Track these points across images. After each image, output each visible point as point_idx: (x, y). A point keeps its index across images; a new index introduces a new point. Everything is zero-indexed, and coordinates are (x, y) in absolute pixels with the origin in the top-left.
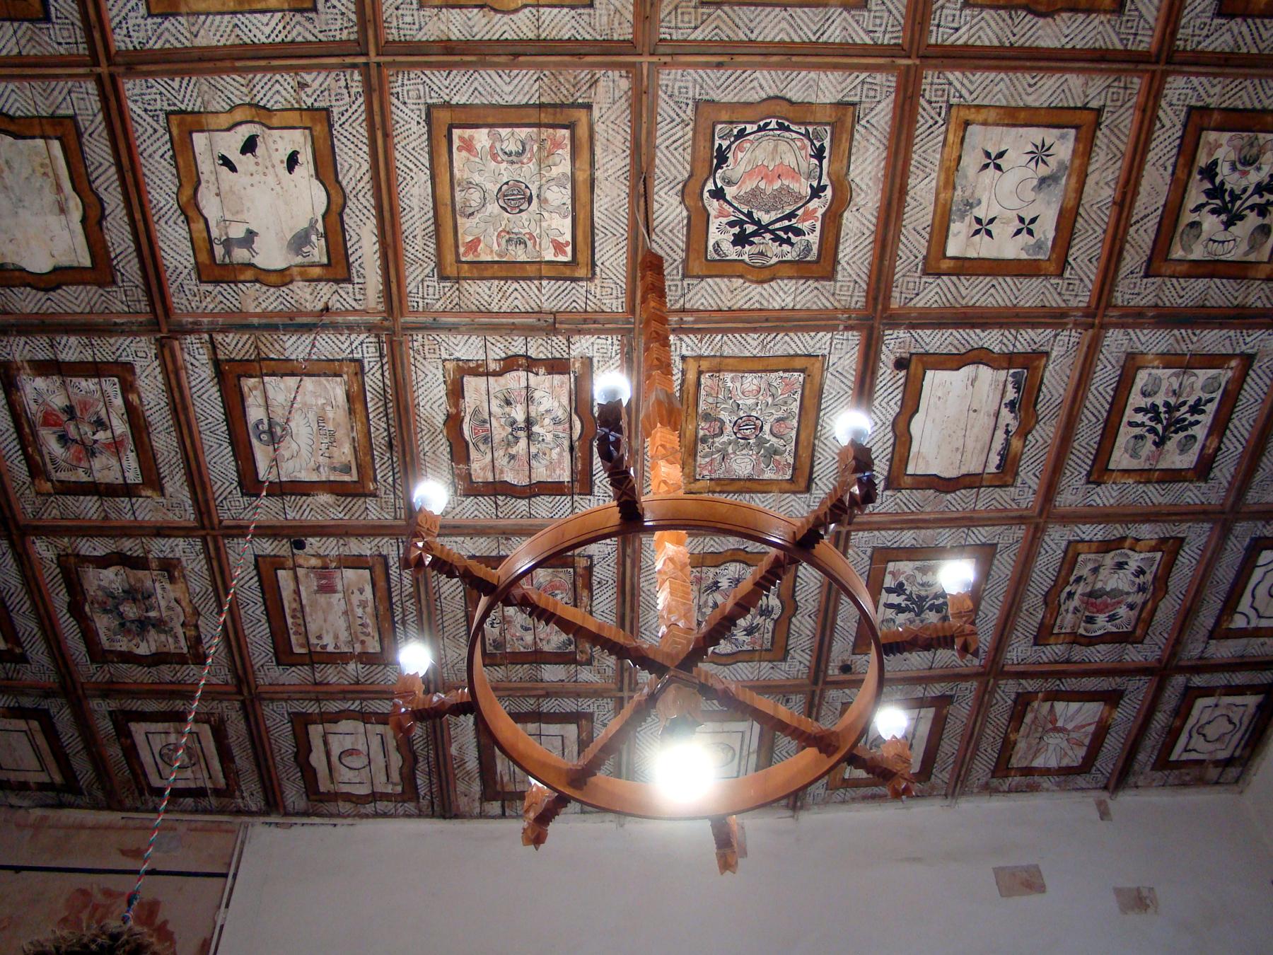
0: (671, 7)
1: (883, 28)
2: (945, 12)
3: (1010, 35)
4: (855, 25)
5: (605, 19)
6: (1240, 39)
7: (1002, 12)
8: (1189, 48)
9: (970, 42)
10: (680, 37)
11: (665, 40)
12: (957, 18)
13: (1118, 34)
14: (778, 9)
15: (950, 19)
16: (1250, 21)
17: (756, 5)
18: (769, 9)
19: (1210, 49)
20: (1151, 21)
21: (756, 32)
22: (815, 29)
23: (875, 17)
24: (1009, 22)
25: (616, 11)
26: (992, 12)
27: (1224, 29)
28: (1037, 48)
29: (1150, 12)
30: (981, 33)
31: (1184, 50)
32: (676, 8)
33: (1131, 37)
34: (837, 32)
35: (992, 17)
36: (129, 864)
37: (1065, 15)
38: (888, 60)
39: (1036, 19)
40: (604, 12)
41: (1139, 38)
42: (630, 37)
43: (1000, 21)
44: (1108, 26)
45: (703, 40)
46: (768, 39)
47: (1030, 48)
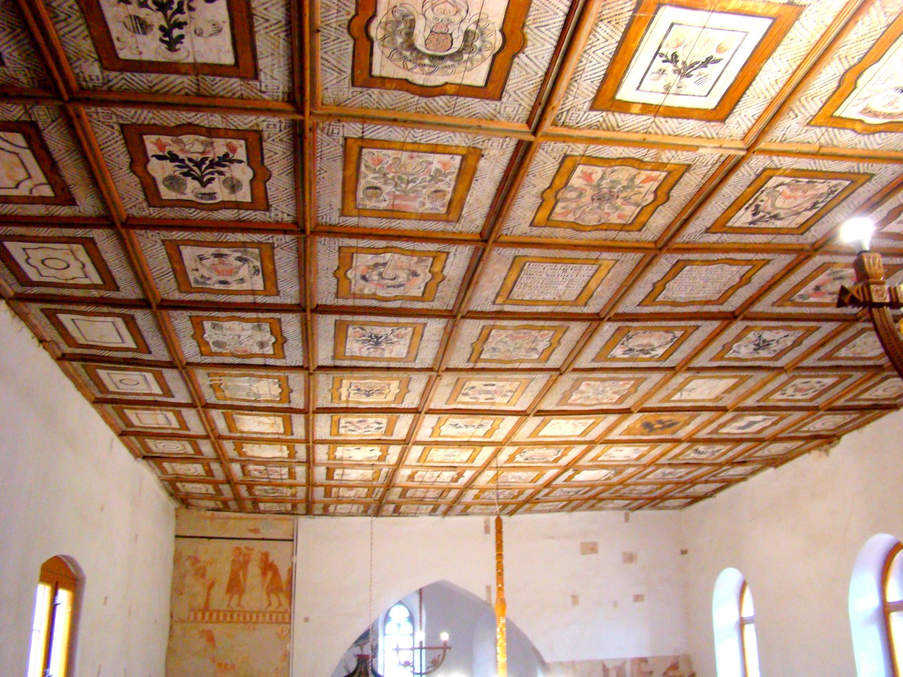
36: (253, 536)
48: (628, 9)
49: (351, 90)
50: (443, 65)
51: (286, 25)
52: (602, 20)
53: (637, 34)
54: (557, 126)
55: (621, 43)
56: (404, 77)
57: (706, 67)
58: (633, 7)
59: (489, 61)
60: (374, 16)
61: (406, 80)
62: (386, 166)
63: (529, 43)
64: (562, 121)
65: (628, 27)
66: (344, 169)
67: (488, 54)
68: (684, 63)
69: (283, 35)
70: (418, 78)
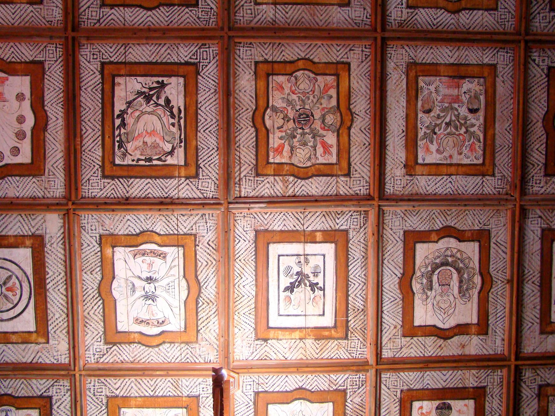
48: (352, 322)
49: (490, 226)
50: (441, 258)
51: (524, 280)
52: (363, 310)
53: (340, 303)
54: (364, 211)
55: (348, 296)
56: (462, 244)
57: (291, 283)
58: (349, 324)
59: (417, 268)
60: (479, 293)
61: (460, 241)
62: (467, 143)
63: (397, 286)
64: (362, 216)
65: (347, 310)
66: (494, 135)
67: (418, 274)
68: (305, 285)
69: (526, 271)
70: (452, 243)
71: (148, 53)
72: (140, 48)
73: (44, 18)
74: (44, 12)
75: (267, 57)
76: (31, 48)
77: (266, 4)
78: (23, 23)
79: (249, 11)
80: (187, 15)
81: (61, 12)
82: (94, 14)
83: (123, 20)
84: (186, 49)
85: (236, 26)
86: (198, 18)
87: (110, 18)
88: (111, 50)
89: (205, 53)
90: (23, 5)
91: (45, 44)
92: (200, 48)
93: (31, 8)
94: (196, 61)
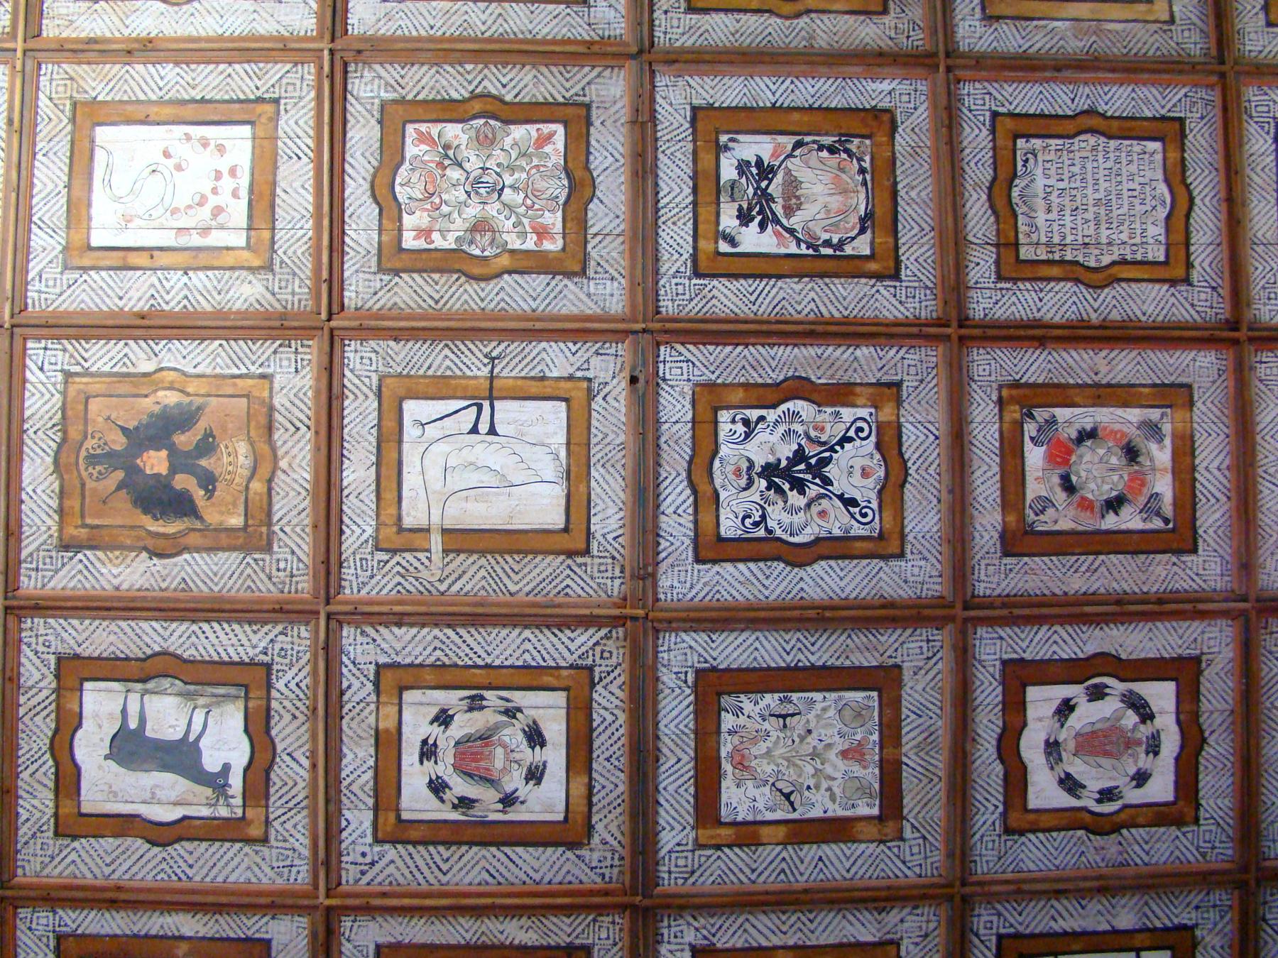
0: (73, 74)
1: (44, 289)
2: (60, 353)
3: (35, 428)
4: (48, 259)
5: (64, 11)
6: (34, 691)
7: (59, 415)
8: (23, 635)
9: (28, 386)
10: (42, 84)
11: (40, 68)
12: (54, 367)
13: (38, 549)
14: (66, 179)
15: (53, 360)
16: (54, 696)
17: (71, 158)
18: (66, 169)
19: (23, 660)
20: (52, 584)
21: (44, 159)
22: (45, 219)
23: (55, 279)
24: (50, 425)
25: (71, 22)
26: (60, 404)
27: (45, 670)
28: (22, 460)
29: (61, 581)
30: (38, 395)
31: (21, 630)
32: (72, 79)
33: (34, 566)
34: (41, 243)
35: (54, 406)
37: (56, 485)
38: (10, 295)
39: (52, 454)
40: (71, 10)
41: (33, 574)
42: (45, 34)
43: (50, 414)
44: (45, 536)
45: (38, 106)
46: (36, 172)
47: (22, 452)
71: (1262, 204)
72: (1256, 220)
73: (1214, 382)
74: (1205, 382)
75: (1259, 7)
76: (1264, 405)
77: (1171, 7)
78: (1224, 419)
79: (1186, 34)
80: (1198, 136)
81: (1202, 353)
82: (1203, 296)
83: (1211, 248)
84: (1254, 141)
85: (1214, 52)
86: (1202, 118)
87: (1208, 269)
88: (1261, 268)
89: (1259, 109)
90: (1195, 418)
91: (1258, 383)
92: (1251, 117)
93: (1199, 404)
94: (1272, 124)
